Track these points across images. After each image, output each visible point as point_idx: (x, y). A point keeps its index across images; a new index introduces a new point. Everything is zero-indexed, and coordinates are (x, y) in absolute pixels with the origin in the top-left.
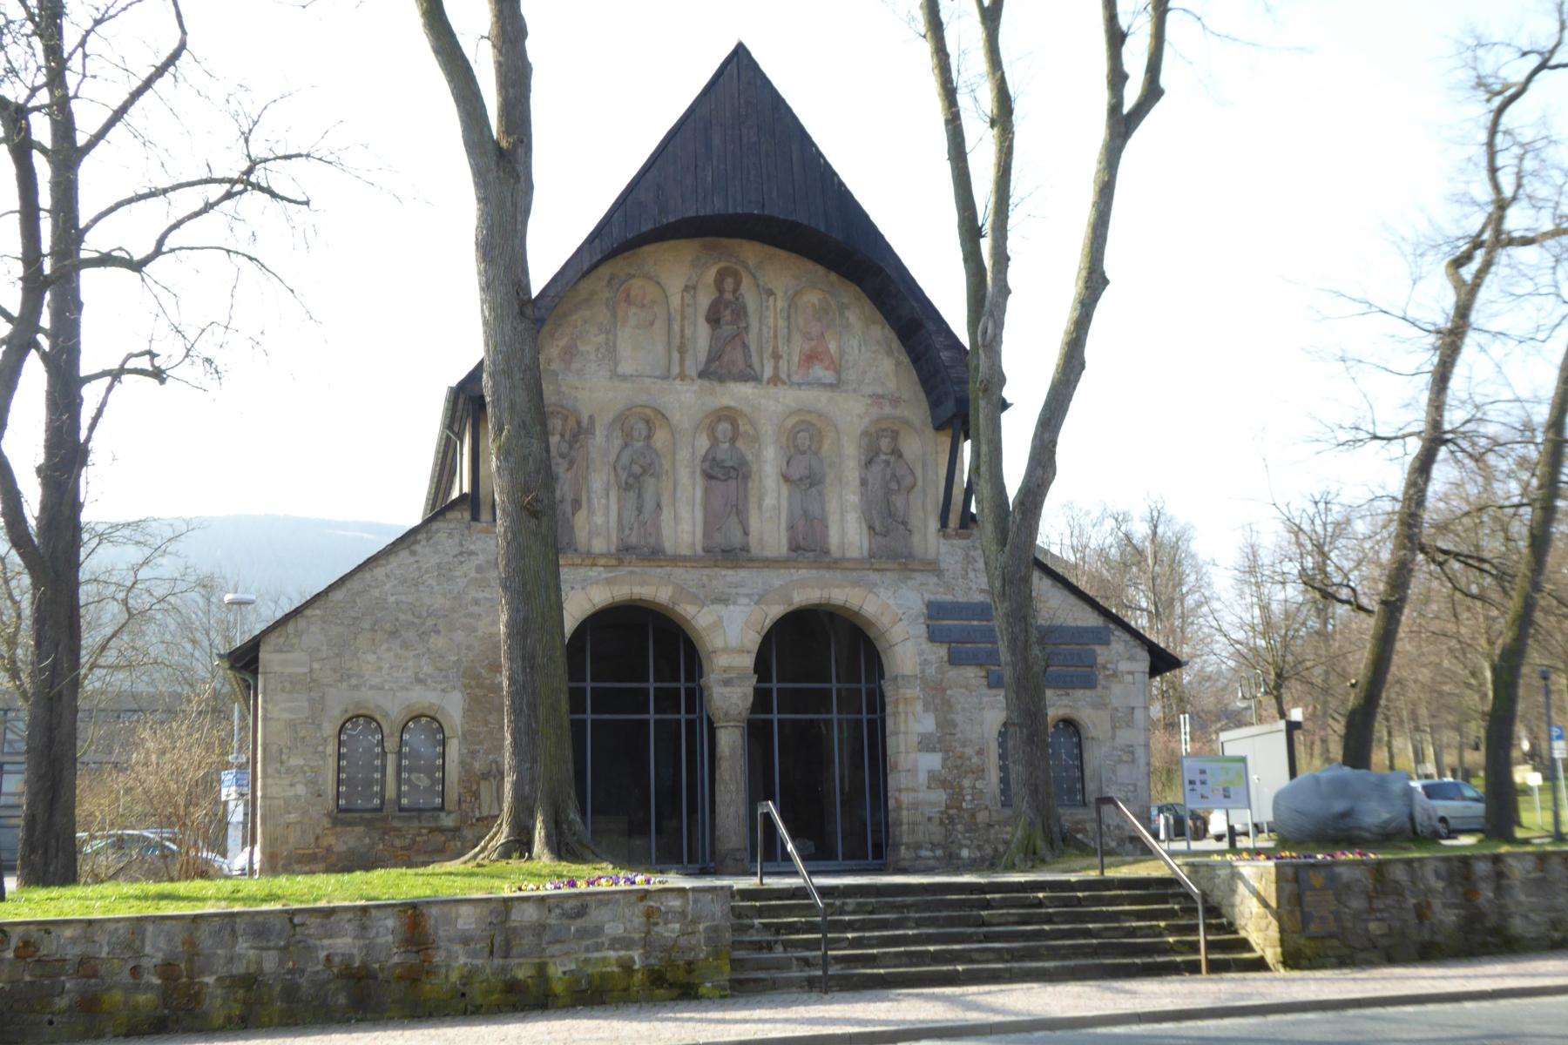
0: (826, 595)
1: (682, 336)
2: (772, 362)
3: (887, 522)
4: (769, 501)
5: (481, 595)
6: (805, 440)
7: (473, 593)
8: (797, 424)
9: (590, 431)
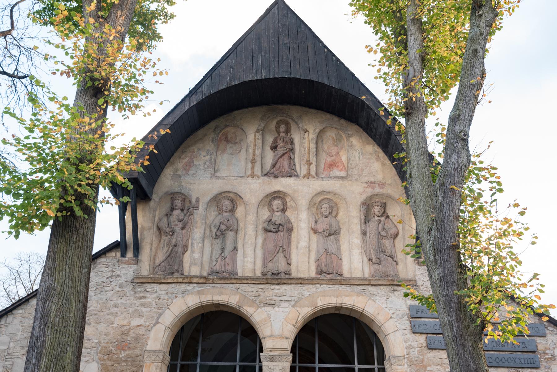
1: (254, 155)
2: (306, 166)
3: (380, 255)
6: (326, 207)
7: (116, 301)
8: (322, 200)
9: (196, 207)
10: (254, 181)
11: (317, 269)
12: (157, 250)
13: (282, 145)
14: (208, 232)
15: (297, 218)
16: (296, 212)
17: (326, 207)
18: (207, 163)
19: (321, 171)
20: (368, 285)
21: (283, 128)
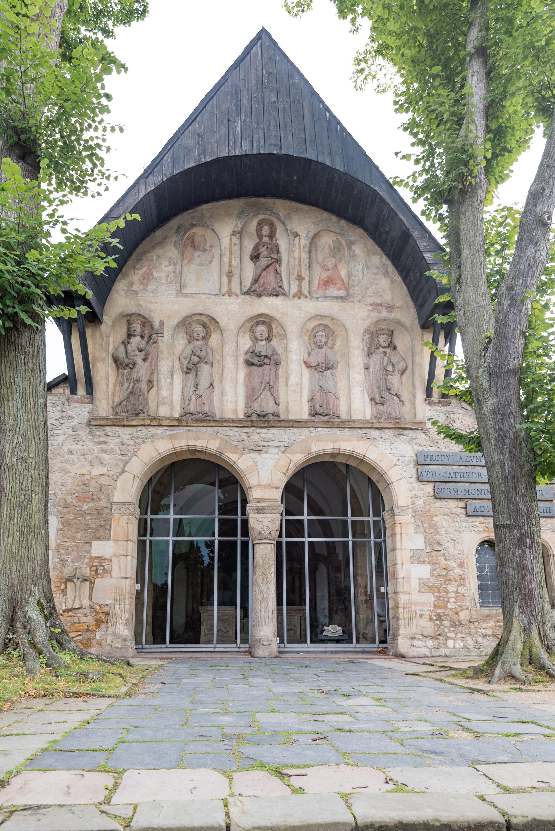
0: (337, 446)
2: (297, 283)
4: (293, 380)
5: (74, 447)
8: (316, 326)
9: (160, 333)
10: (232, 301)
11: (310, 410)
12: (115, 386)
13: (265, 253)
14: (177, 365)
15: (286, 348)
16: (285, 341)
17: (323, 333)
18: (171, 276)
19: (315, 289)
20: (370, 428)
21: (266, 230)
